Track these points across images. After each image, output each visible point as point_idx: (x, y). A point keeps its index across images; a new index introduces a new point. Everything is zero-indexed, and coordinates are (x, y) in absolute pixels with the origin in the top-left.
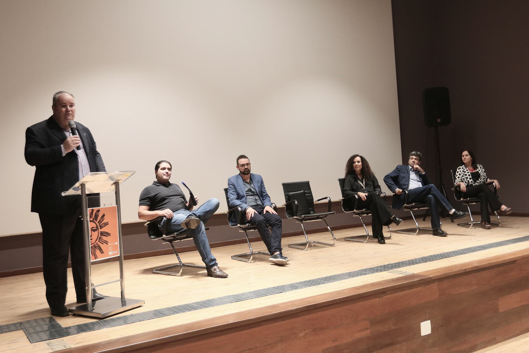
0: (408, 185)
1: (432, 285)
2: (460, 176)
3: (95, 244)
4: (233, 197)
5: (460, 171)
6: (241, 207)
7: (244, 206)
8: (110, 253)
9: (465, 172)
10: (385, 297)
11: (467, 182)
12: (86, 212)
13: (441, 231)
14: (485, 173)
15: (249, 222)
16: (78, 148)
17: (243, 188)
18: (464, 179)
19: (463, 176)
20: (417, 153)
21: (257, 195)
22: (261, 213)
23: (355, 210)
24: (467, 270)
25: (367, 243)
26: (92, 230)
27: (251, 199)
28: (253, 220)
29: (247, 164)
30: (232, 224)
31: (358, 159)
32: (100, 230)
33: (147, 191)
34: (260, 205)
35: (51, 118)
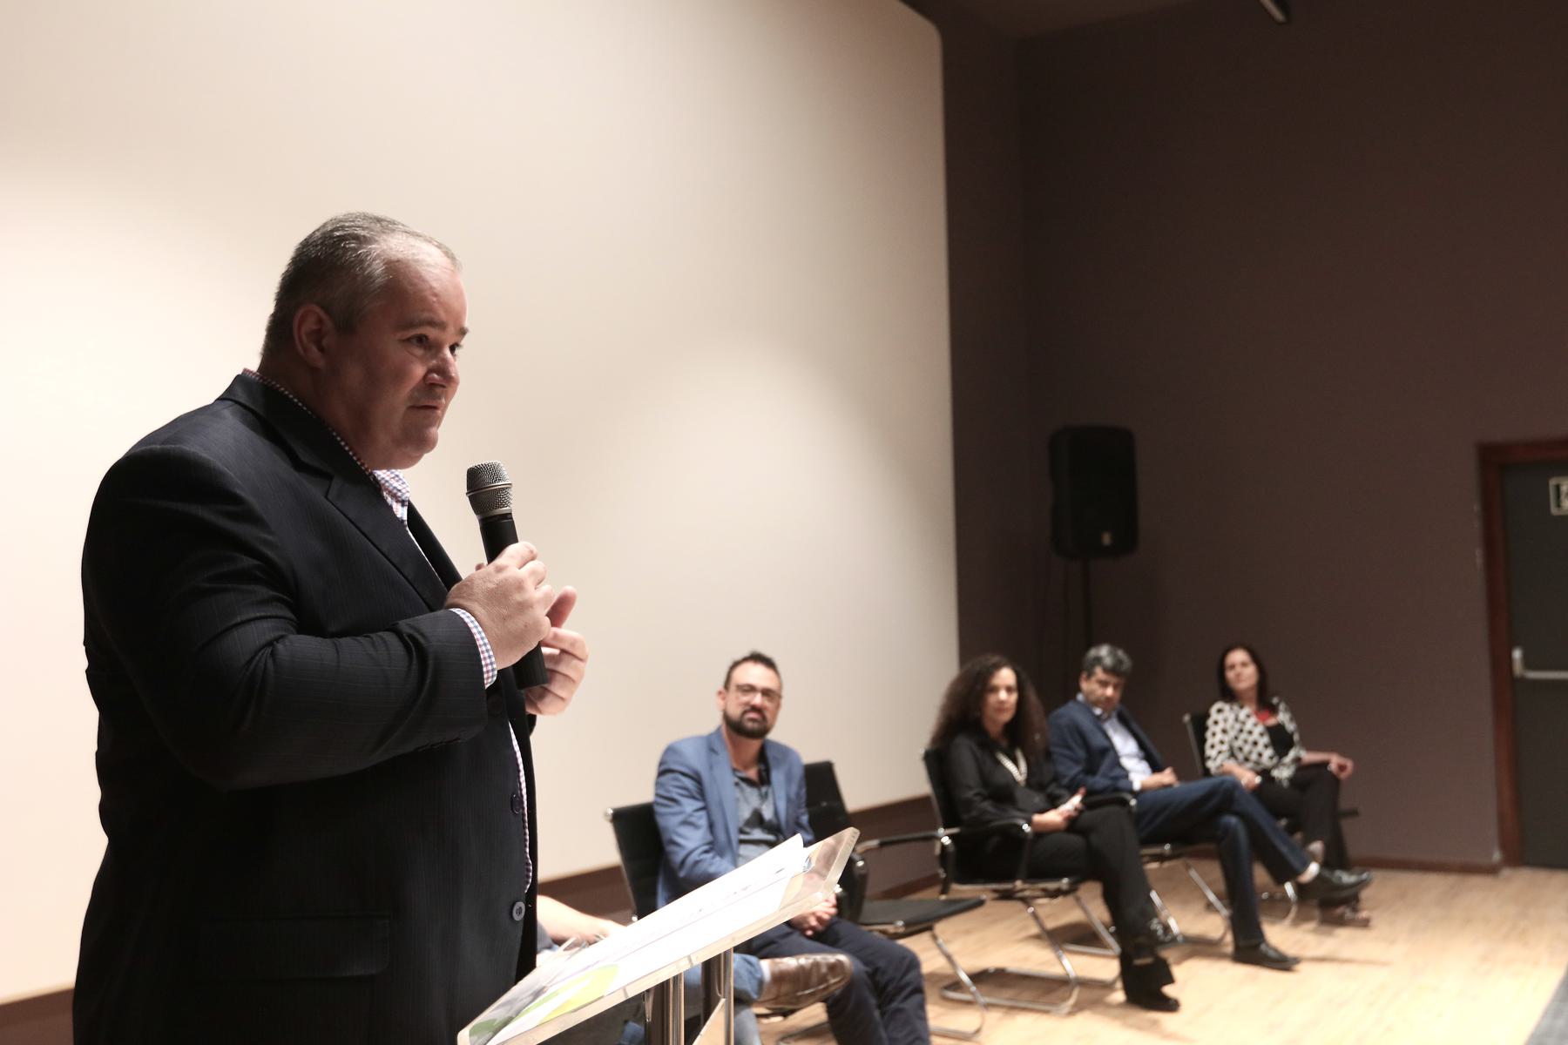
2: (1226, 738)
29: (766, 693)
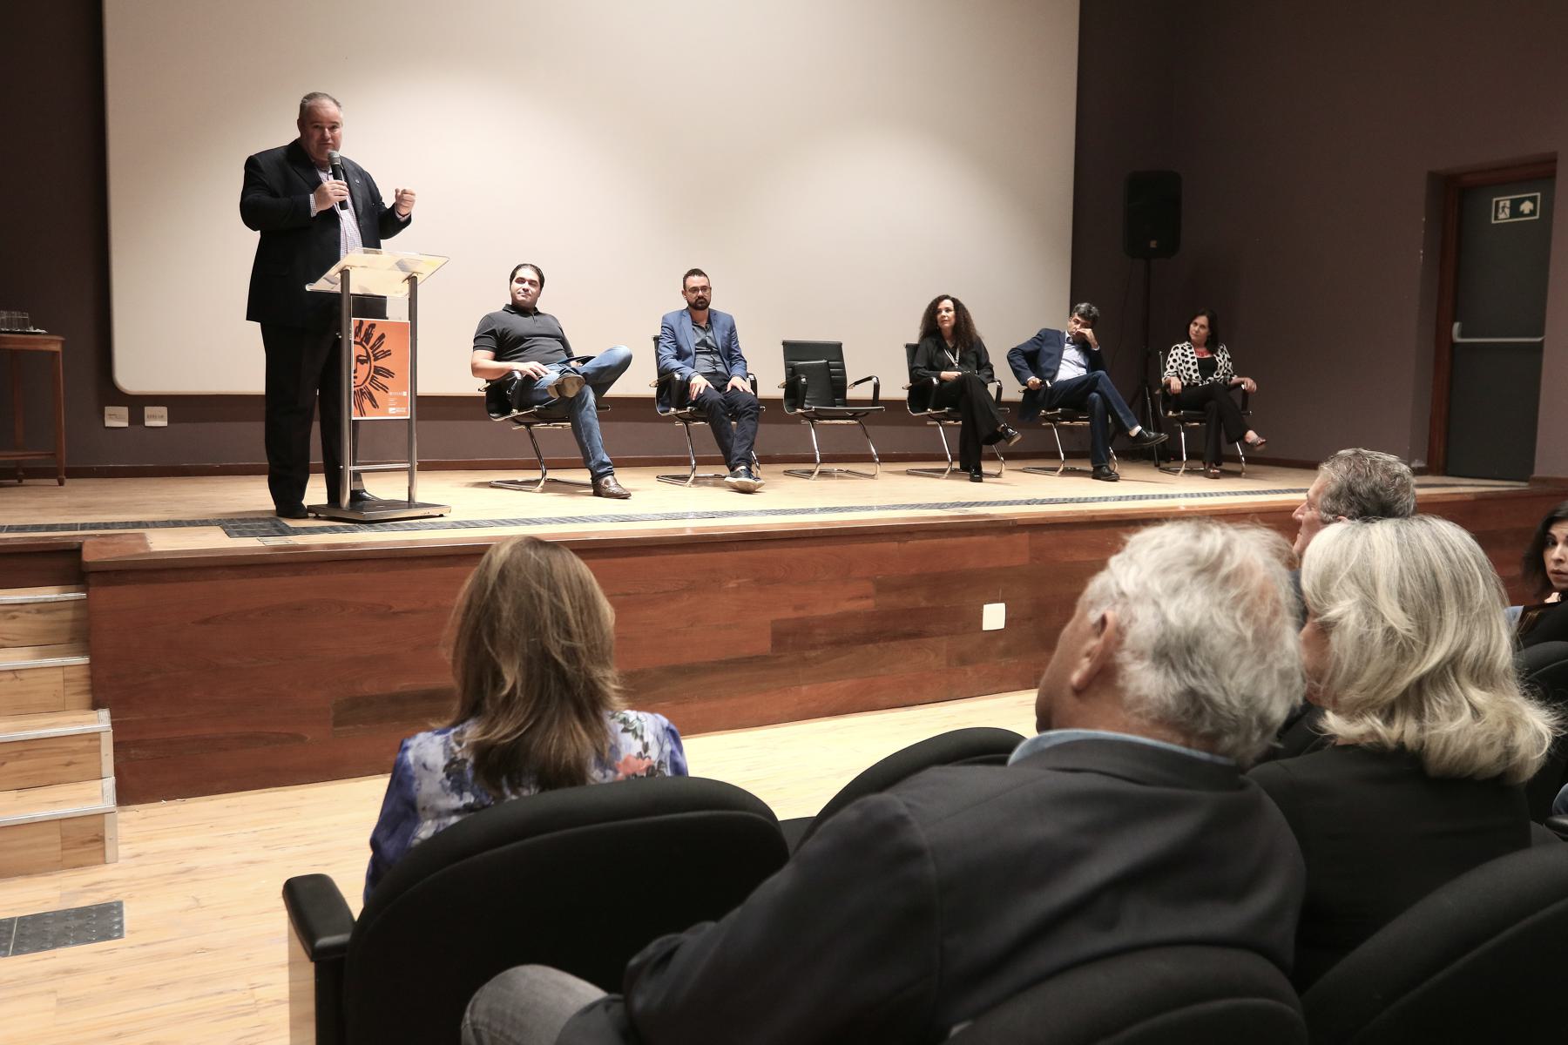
0: (1056, 373)
1: (1016, 535)
2: (1175, 365)
3: (362, 387)
4: (668, 353)
5: (1177, 354)
6: (681, 374)
7: (688, 371)
8: (391, 410)
9: (1186, 356)
10: (912, 542)
11: (1188, 377)
12: (349, 326)
13: (1109, 469)
14: (1230, 364)
15: (693, 404)
16: (343, 205)
17: (691, 338)
18: (1182, 371)
19: (1180, 365)
20: (1090, 312)
21: (718, 353)
22: (720, 389)
23: (929, 410)
24: (1098, 519)
25: (947, 478)
26: (358, 360)
27: (704, 362)
28: (700, 401)
29: (704, 288)
30: (663, 409)
31: (948, 303)
32: (373, 363)
33: (489, 319)
34: (722, 373)
35: (296, 142)
